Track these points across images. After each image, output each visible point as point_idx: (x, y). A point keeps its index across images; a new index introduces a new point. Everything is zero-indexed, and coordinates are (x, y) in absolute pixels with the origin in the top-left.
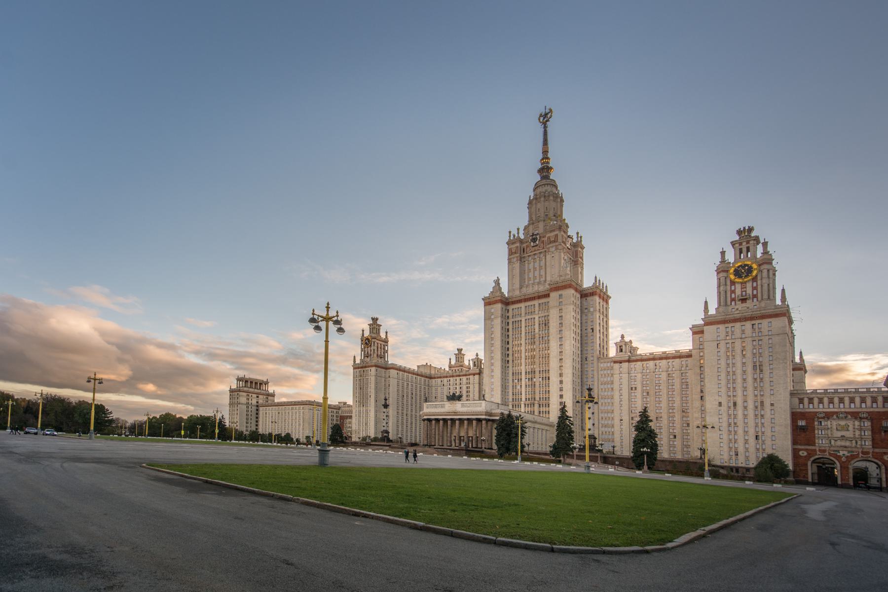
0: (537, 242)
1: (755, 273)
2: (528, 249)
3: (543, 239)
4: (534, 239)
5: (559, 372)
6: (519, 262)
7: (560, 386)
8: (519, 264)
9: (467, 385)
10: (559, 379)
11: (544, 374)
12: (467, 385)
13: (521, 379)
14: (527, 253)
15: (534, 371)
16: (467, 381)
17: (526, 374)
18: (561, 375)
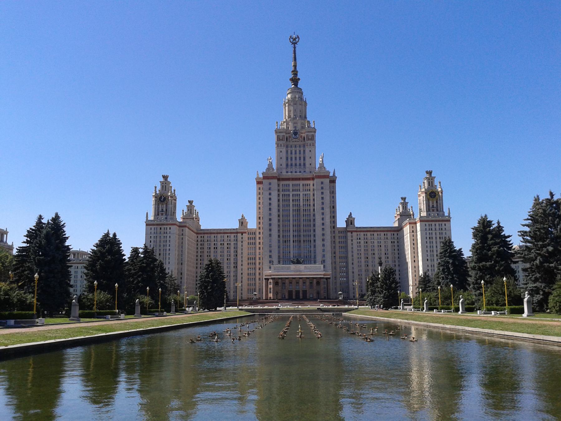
0: (297, 136)
1: (437, 196)
2: (290, 139)
3: (302, 135)
4: (296, 132)
5: (322, 238)
6: (285, 147)
7: (322, 248)
8: (285, 149)
9: (235, 242)
10: (322, 243)
11: (307, 238)
12: (235, 242)
13: (290, 241)
14: (289, 142)
15: (300, 235)
16: (234, 238)
17: (293, 237)
18: (323, 240)
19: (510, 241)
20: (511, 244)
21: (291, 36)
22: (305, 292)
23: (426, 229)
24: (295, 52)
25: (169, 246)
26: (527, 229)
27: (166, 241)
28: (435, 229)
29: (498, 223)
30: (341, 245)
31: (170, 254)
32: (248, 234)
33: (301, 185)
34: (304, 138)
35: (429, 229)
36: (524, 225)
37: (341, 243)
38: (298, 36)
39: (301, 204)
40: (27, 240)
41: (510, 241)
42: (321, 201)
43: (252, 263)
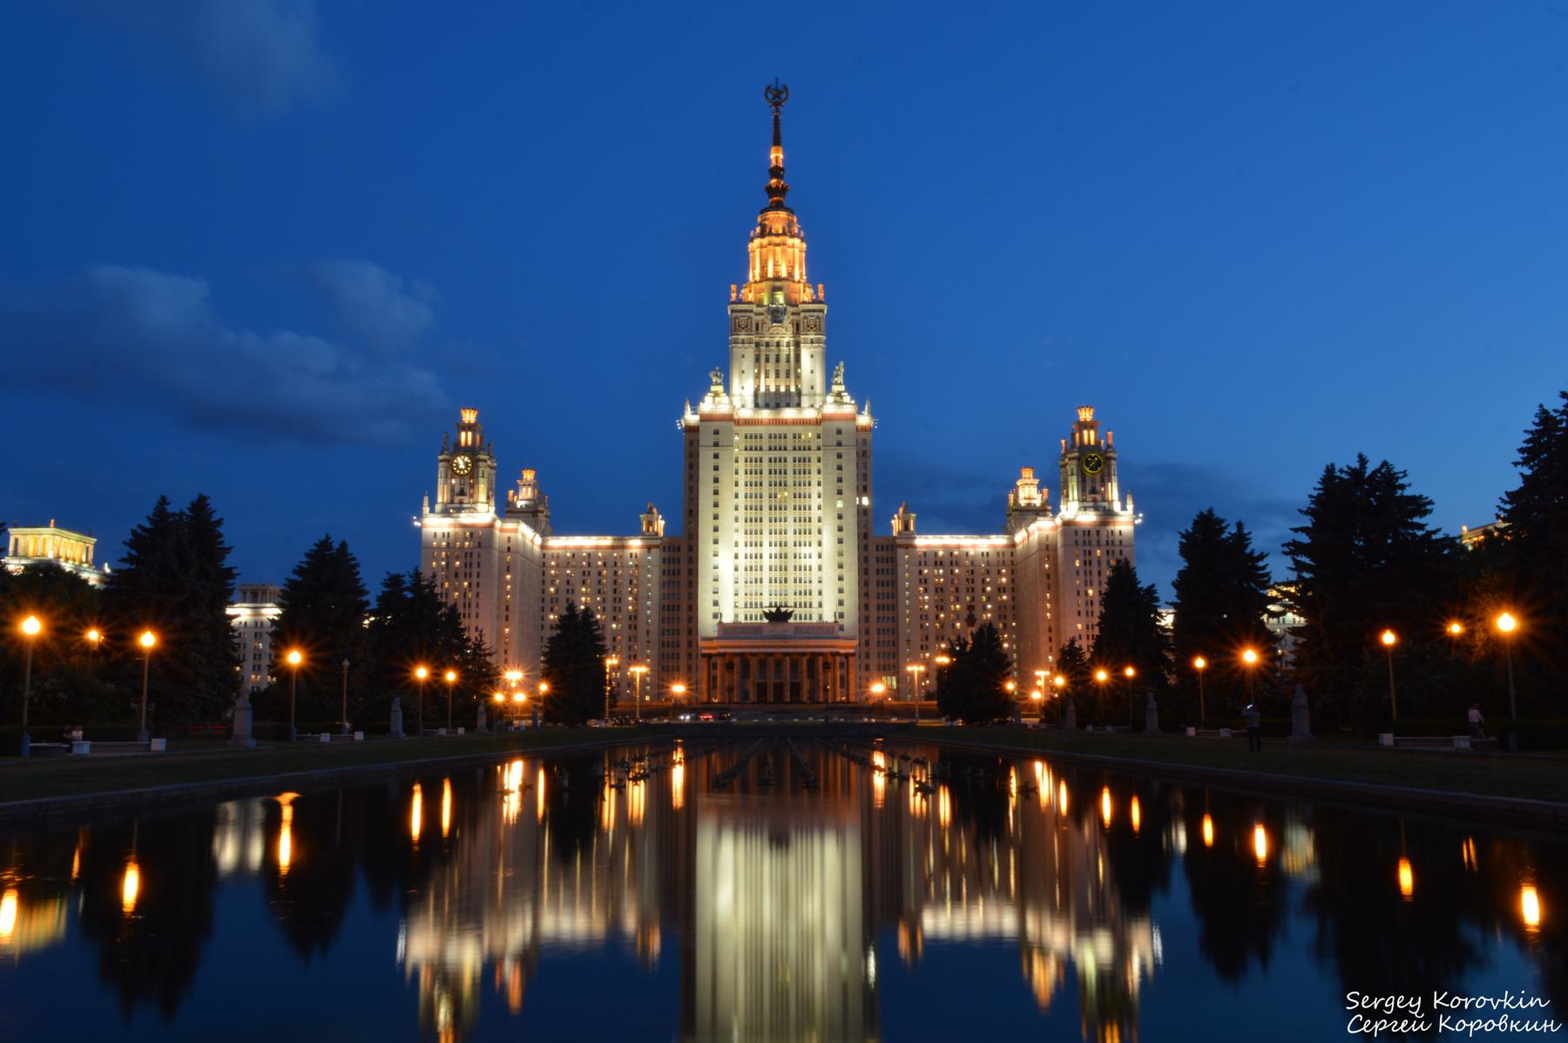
8: (752, 350)
19: (1264, 568)
20: (1267, 574)
21: (769, 87)
22: (796, 688)
23: (1077, 542)
24: (777, 121)
25: (478, 575)
26: (1304, 539)
27: (471, 564)
28: (1099, 542)
29: (1240, 526)
30: (881, 577)
31: (480, 596)
32: (664, 551)
33: (790, 436)
34: (798, 325)
35: (1085, 542)
36: (1296, 530)
37: (883, 573)
38: (785, 88)
39: (790, 482)
40: (129, 554)
41: (1264, 568)
42: (836, 473)
43: (673, 618)
